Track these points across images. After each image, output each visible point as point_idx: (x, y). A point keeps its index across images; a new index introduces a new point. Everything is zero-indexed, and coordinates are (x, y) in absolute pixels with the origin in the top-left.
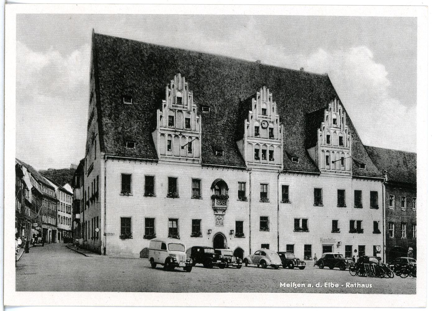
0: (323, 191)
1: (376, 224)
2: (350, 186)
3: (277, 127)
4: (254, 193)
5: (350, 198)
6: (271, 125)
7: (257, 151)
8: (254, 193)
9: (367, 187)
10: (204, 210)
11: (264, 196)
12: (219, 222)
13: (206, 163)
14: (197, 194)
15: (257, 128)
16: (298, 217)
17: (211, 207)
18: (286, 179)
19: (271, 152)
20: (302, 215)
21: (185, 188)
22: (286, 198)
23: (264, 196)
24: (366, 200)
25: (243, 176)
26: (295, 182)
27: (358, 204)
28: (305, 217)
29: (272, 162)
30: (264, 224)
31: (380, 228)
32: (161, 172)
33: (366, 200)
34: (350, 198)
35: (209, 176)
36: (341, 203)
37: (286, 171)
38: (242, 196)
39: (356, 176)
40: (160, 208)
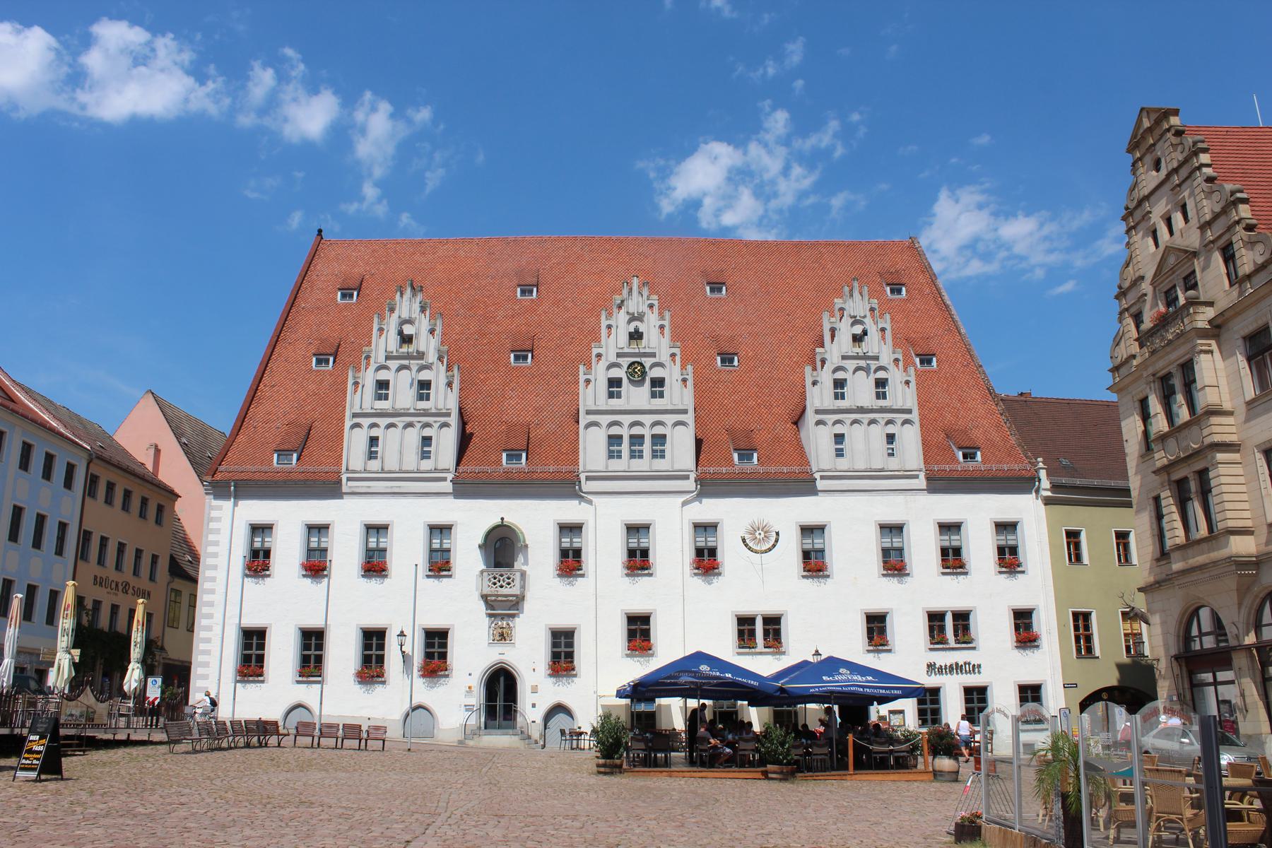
0: (833, 530)
1: (1023, 618)
2: (923, 513)
3: (672, 374)
4: (604, 550)
5: (923, 549)
6: (656, 373)
7: (614, 440)
8: (604, 550)
9: (978, 513)
10: (458, 603)
11: (638, 561)
12: (503, 636)
13: (466, 487)
14: (440, 565)
15: (614, 383)
16: (746, 609)
17: (476, 596)
18: (710, 509)
19: (659, 439)
20: (758, 607)
21: (407, 551)
22: (706, 561)
23: (638, 561)
24: (980, 547)
25: (568, 510)
26: (734, 515)
27: (952, 559)
28: (771, 609)
29: (660, 465)
30: (639, 630)
31: (1047, 624)
32: (345, 517)
33: (980, 547)
34: (923, 549)
35: (474, 518)
36: (894, 564)
37: (710, 486)
38: (570, 562)
39: (940, 483)
40: (347, 605)
